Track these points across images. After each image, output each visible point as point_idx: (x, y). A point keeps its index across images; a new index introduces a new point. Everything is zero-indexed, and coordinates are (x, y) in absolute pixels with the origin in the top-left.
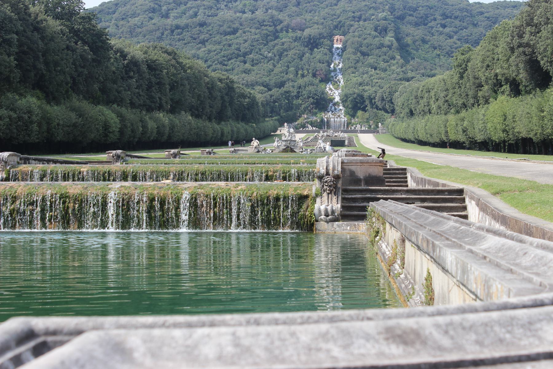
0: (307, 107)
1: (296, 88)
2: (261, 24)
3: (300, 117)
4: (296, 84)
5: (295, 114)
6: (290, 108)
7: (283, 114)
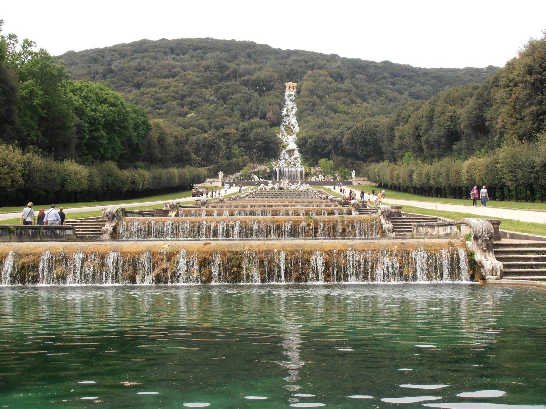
2: (207, 69)
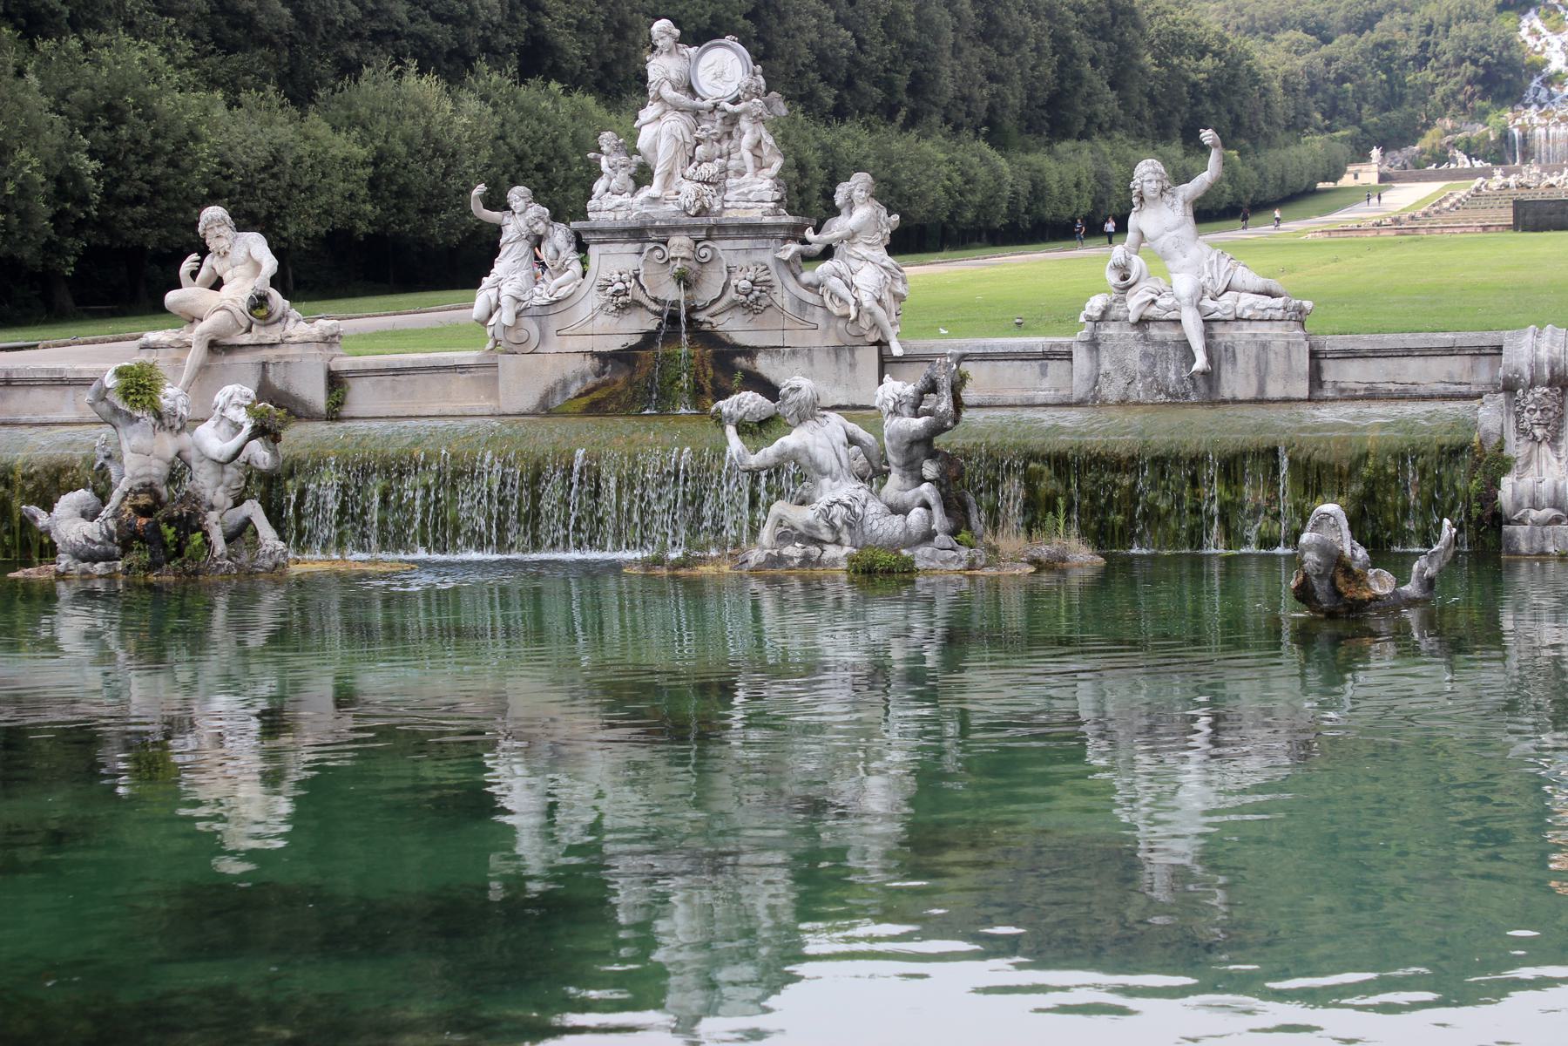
0: (1454, 94)
1: (1414, 33)
3: (1427, 126)
4: (1415, 18)
5: (1412, 116)
6: (1393, 98)
7: (1371, 118)
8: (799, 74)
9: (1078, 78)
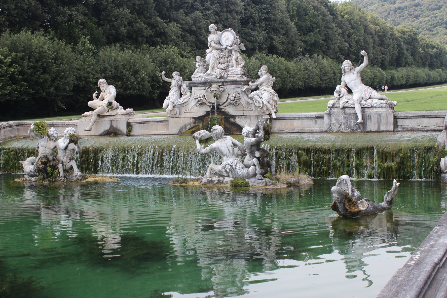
8: (336, 53)
9: (403, 54)
